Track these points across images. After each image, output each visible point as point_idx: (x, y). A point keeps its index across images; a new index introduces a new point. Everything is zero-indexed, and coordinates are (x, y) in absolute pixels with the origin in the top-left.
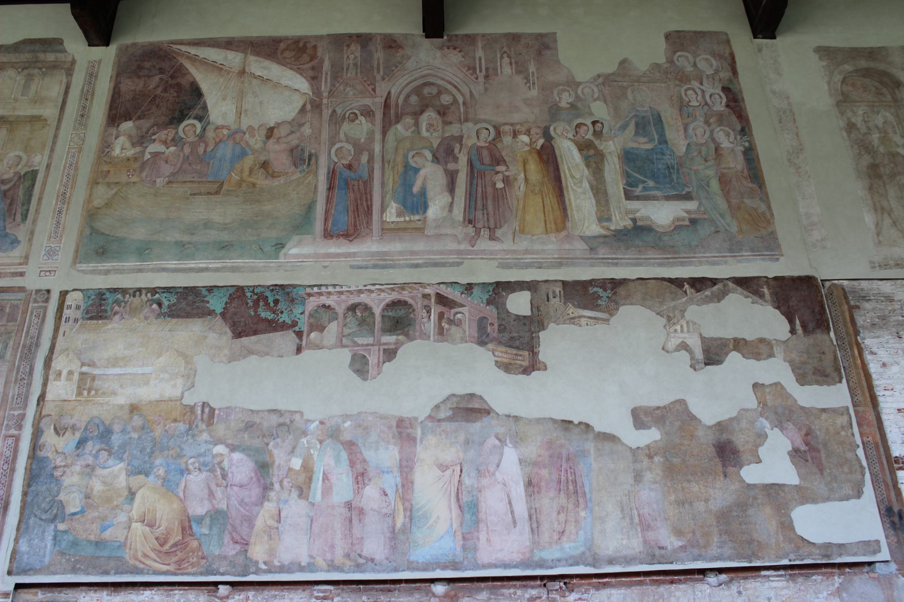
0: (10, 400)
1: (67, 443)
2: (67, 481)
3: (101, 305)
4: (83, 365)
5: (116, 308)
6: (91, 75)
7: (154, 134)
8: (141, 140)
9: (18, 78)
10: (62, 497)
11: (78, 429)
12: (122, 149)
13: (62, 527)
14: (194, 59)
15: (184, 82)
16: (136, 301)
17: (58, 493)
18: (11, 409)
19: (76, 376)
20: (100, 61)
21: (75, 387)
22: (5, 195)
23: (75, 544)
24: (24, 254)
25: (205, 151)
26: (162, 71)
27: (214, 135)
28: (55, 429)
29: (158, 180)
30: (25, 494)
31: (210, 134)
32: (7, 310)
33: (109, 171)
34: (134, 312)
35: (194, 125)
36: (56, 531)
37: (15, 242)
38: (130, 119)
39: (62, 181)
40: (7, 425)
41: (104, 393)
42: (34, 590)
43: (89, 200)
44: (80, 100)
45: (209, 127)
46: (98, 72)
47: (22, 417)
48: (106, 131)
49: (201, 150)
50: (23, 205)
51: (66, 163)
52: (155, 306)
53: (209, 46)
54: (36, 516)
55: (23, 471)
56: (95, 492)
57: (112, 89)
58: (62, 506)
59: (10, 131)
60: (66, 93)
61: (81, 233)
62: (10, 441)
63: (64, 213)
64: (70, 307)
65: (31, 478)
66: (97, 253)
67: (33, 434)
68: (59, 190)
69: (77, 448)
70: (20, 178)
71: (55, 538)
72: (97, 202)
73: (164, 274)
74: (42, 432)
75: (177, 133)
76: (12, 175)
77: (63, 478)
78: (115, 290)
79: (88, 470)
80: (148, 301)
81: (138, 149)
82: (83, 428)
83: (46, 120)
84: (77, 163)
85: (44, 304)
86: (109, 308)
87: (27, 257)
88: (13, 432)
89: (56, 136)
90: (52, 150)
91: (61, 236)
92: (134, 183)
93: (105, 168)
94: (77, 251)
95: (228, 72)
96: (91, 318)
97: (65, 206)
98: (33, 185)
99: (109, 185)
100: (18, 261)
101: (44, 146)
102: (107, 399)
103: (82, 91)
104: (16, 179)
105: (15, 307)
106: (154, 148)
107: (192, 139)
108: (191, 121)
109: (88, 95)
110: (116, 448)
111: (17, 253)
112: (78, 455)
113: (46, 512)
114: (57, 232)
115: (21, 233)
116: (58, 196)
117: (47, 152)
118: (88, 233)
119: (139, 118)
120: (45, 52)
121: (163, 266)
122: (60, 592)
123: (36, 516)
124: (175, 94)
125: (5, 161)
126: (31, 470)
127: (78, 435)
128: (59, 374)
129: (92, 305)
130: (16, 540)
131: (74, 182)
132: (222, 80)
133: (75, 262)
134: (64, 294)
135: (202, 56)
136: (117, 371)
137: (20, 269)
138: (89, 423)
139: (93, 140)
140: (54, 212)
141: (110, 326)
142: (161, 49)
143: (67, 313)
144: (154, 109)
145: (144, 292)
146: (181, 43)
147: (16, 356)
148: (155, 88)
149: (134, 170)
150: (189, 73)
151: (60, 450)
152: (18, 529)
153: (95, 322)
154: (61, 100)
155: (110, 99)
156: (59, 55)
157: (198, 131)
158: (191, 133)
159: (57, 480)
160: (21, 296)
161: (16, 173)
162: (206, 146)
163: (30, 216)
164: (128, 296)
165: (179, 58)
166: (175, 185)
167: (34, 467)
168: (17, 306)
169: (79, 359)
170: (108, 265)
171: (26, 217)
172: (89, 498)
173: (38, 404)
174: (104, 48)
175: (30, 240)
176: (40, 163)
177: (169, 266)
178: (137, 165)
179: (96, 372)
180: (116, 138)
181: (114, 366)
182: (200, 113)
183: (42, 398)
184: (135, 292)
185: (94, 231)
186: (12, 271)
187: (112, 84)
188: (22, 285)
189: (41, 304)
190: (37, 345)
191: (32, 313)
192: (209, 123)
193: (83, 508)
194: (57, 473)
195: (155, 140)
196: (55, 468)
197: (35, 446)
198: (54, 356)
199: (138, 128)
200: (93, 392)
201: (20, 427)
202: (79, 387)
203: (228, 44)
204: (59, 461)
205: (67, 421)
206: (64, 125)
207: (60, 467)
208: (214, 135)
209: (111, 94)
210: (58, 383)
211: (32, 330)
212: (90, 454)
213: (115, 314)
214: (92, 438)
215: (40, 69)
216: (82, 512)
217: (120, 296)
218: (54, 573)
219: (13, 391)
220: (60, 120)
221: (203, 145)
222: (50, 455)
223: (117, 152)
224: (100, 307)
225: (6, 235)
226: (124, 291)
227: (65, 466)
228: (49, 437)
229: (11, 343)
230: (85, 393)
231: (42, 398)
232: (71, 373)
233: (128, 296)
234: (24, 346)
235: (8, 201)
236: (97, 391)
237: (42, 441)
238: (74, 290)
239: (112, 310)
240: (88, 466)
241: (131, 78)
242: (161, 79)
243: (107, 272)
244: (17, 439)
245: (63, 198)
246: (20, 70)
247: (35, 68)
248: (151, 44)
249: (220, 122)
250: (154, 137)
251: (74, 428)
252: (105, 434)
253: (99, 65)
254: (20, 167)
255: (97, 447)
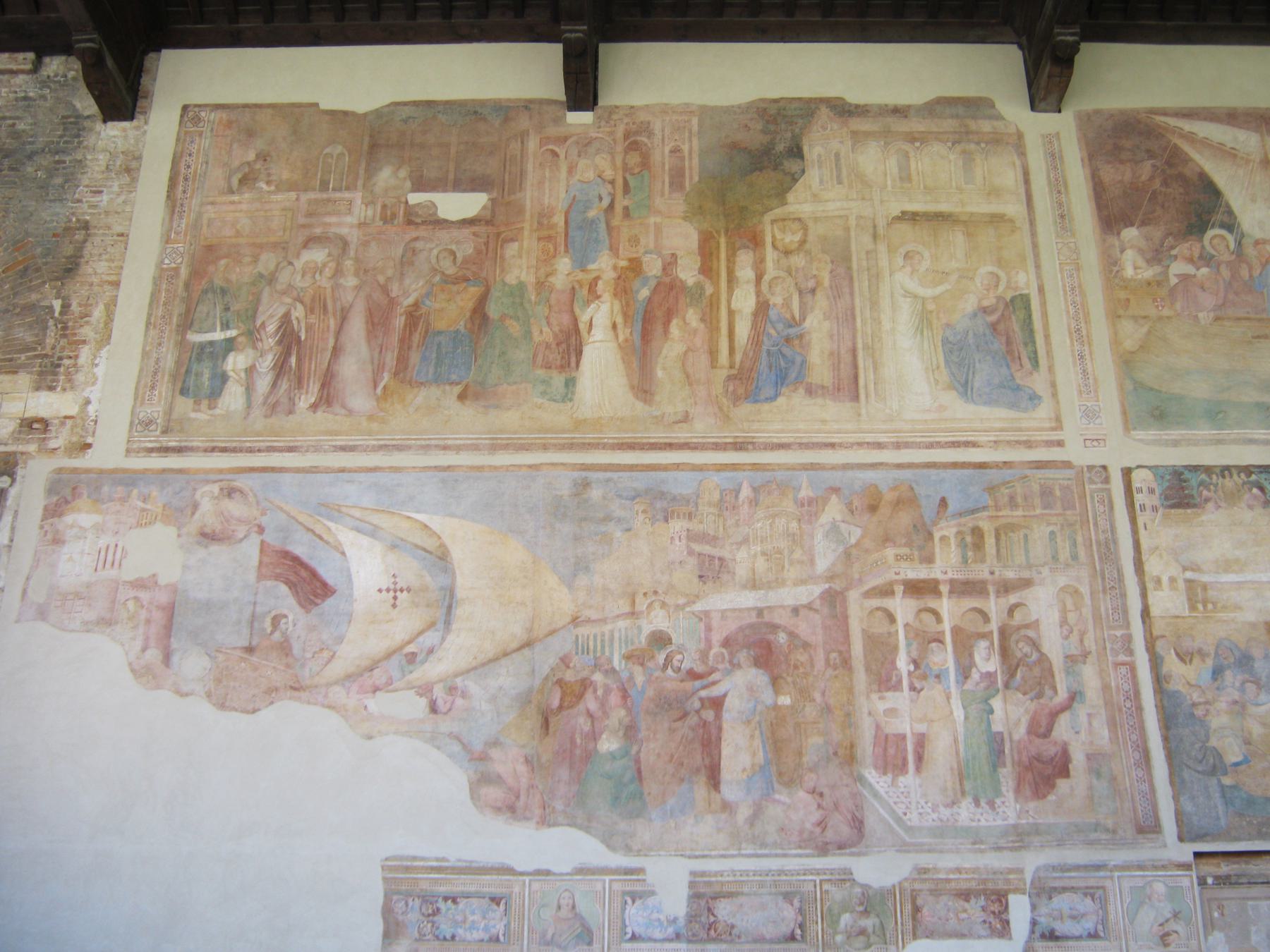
0: (1104, 616)
1: (1197, 672)
2: (1215, 722)
3: (1183, 488)
4: (1185, 569)
5: (1205, 493)
6: (1053, 155)
7: (1172, 248)
8: (1157, 256)
9: (952, 157)
10: (1213, 742)
11: (1208, 655)
12: (1136, 268)
13: (1227, 781)
14: (1190, 138)
15: (1187, 172)
16: (1228, 483)
17: (1208, 738)
18: (1110, 628)
19: (1181, 585)
20: (1058, 134)
21: (1184, 598)
22: (995, 329)
23: (1251, 801)
24: (1053, 415)
25: (1251, 276)
26: (1151, 154)
27: (1255, 253)
28: (1177, 654)
29: (1201, 315)
30: (1166, 739)
31: (1250, 251)
32: (1058, 493)
33: (1128, 300)
34: (1232, 498)
35: (1223, 238)
36: (1222, 788)
37: (1034, 398)
38: (1132, 225)
39: (1068, 312)
40: (1112, 649)
41: (1225, 608)
42: (1215, 861)
43: (1115, 342)
44: (1051, 192)
45: (1244, 241)
46: (1061, 151)
47: (1128, 639)
48: (1104, 241)
49: (1245, 273)
50: (1026, 344)
51: (1064, 286)
52: (1255, 491)
53: (1205, 119)
54: (1188, 767)
55: (1154, 709)
56: (1255, 736)
57: (1089, 176)
58: (1219, 756)
59: (969, 235)
60: (1027, 182)
61: (1121, 387)
62: (1123, 670)
63: (1087, 357)
64: (1140, 490)
65: (1167, 722)
66: (1153, 416)
67: (1150, 660)
68: (1069, 326)
69: (1214, 678)
70: (1007, 305)
71: (1223, 796)
72: (1129, 344)
73: (1254, 447)
74: (1162, 659)
75: (1203, 247)
76: (994, 301)
77: (1208, 718)
78: (1195, 469)
79: (1237, 708)
80: (1244, 483)
81: (1158, 269)
82: (1212, 652)
83: (1012, 221)
84: (1080, 286)
85: (1104, 486)
86: (1194, 492)
87: (1058, 419)
88: (1122, 658)
89: (1035, 246)
90: (1038, 267)
91: (1096, 391)
92: (1168, 318)
93: (1123, 295)
94: (1124, 413)
95: (1248, 161)
96: (1172, 507)
97: (1086, 348)
98: (1030, 316)
99: (1135, 318)
100: (1047, 425)
101: (1023, 259)
102: (1232, 615)
103: (1049, 182)
104: (1001, 306)
105: (1066, 489)
106: (1178, 268)
107: (1226, 257)
108: (1217, 231)
109: (1059, 186)
110: (1264, 679)
111: (1043, 412)
112: (1218, 689)
113: (1201, 762)
114: (1088, 385)
115: (1038, 382)
116: (1070, 333)
117: (1031, 269)
118: (1131, 387)
119: (1143, 223)
120: (974, 118)
121: (1250, 436)
122: (1247, 863)
123: (1188, 767)
124: (1181, 190)
125: (978, 281)
126: (1163, 707)
127: (1210, 662)
128: (1158, 581)
129: (1169, 488)
130: (1176, 798)
131: (1087, 315)
132: (1241, 172)
133: (1127, 429)
134: (1127, 473)
135: (1201, 135)
136: (1232, 577)
137: (1055, 436)
138: (1217, 647)
139: (1091, 256)
140: (1073, 356)
141: (1204, 518)
142: (1139, 122)
143: (1139, 499)
144: (1159, 212)
145: (1234, 472)
146: (1164, 112)
147: (1092, 556)
148: (1152, 178)
149: (1162, 299)
150: (1191, 160)
151: (1193, 682)
152: (1172, 783)
153: (1181, 511)
154: (1022, 190)
155: (1092, 193)
156: (996, 123)
157: (1232, 246)
158: (1222, 248)
159: (1202, 722)
160: (1069, 473)
161: (999, 298)
162: (1251, 269)
163: (1043, 361)
164: (1214, 477)
165: (1168, 135)
166: (1227, 323)
167: (1166, 704)
168: (1068, 487)
169: (1177, 561)
170: (1175, 433)
171: (1037, 362)
172: (1249, 743)
173: (1144, 622)
174: (1056, 115)
175: (1054, 395)
176: (1028, 285)
177: (1256, 437)
178: (1164, 292)
179: (1205, 578)
180: (1122, 251)
181: (1226, 571)
182: (1226, 219)
183: (1145, 613)
184: (1222, 471)
185: (1139, 386)
186: (1045, 438)
187: (1088, 171)
188: (1066, 459)
189: (1100, 486)
190: (1115, 542)
191: (1092, 498)
192: (1243, 235)
193: (1245, 757)
194: (1199, 712)
195: (1176, 257)
196: (1194, 705)
197: (1159, 680)
198: (1144, 558)
199: (1148, 238)
200: (1210, 606)
201: (1130, 652)
202: (1189, 599)
203: (1231, 117)
204: (1196, 697)
205: (1187, 644)
206: (1040, 229)
207: (1200, 704)
208: (1255, 253)
209: (1091, 184)
210: (1160, 593)
211: (1101, 522)
212: (1233, 687)
213: (1207, 500)
214: (1229, 667)
215: (978, 143)
216: (1246, 761)
217: (1203, 476)
218: (1237, 839)
219: (1106, 604)
220: (1032, 222)
221: (1244, 266)
222: (1180, 688)
223: (1129, 272)
224: (1181, 491)
225: (1019, 388)
226: (1208, 470)
227: (1207, 703)
228: (1172, 665)
229: (1080, 539)
230: (1200, 607)
231: (1145, 613)
232: (1172, 580)
233: (1214, 477)
234: (1098, 543)
235: (1004, 339)
236: (1214, 604)
237: (1165, 670)
238: (1139, 467)
239: (1200, 495)
240: (1235, 702)
241: (1109, 162)
242: (1153, 166)
243: (1176, 443)
244: (1132, 668)
245: (1080, 335)
246: (950, 144)
247: (969, 141)
248: (1122, 112)
249: (1258, 234)
250: (1174, 252)
251: (1202, 654)
252: (1245, 661)
253: (1059, 139)
254: (1001, 288)
255: (1239, 677)
